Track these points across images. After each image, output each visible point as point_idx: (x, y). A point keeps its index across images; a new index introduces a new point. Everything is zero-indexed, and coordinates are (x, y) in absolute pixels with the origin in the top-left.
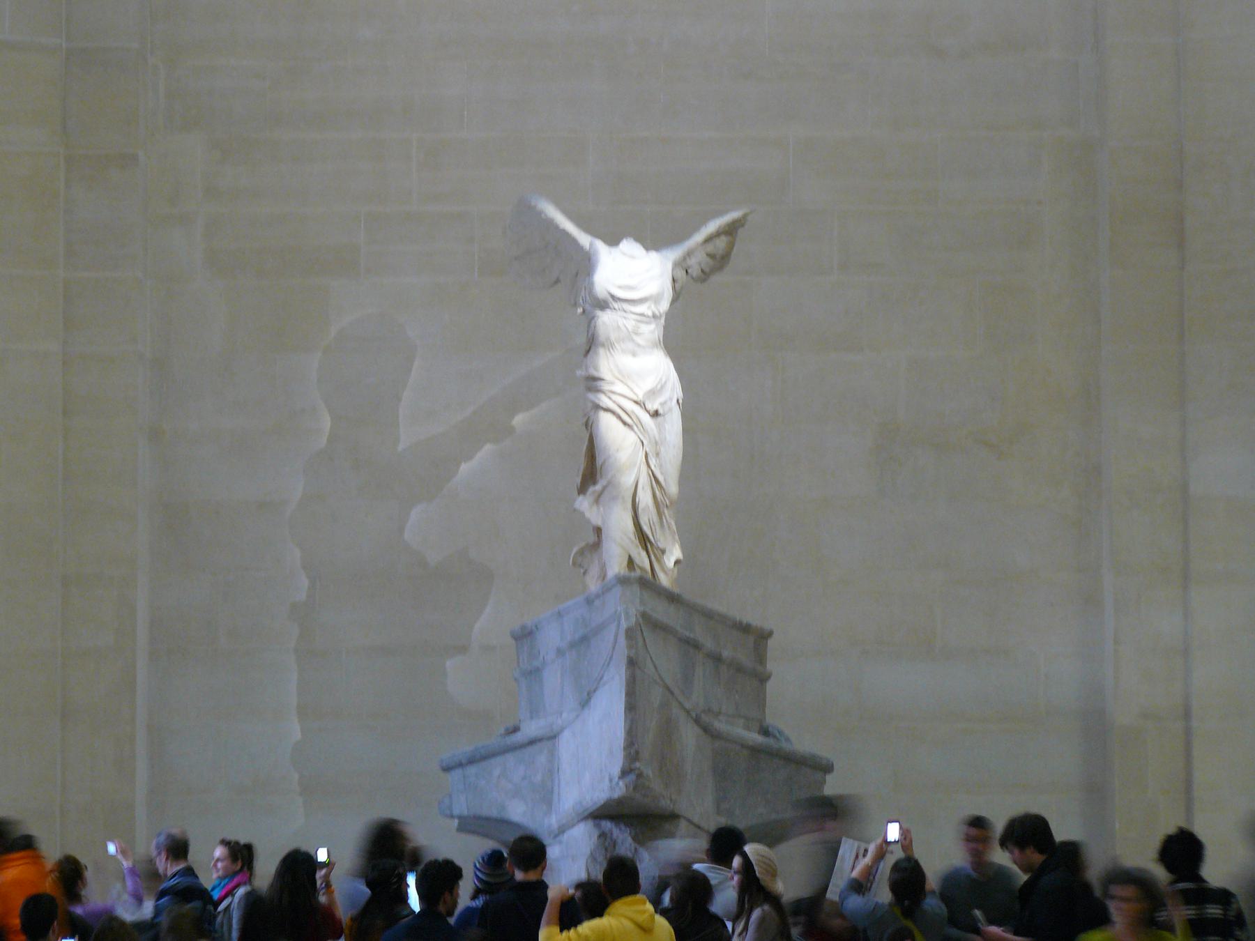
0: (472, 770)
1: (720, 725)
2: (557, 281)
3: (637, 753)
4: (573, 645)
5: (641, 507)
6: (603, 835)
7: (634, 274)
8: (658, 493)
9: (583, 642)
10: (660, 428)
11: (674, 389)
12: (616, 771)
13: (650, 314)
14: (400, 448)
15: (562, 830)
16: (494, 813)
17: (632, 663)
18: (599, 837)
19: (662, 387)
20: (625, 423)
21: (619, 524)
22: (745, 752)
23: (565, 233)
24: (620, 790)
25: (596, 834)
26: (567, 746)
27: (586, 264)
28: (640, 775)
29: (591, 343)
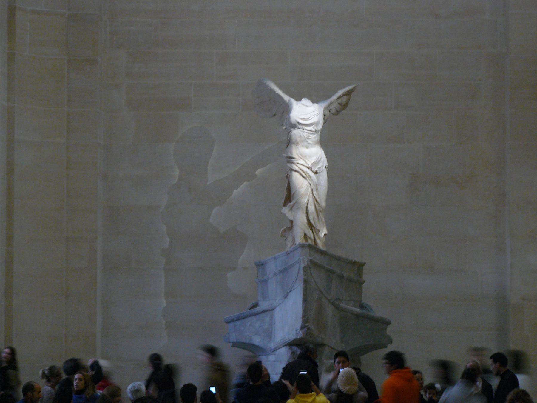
0: (238, 323)
1: (342, 305)
2: (275, 115)
3: (307, 319)
4: (281, 272)
5: (310, 212)
7: (307, 113)
8: (317, 206)
9: (285, 271)
10: (318, 179)
11: (324, 162)
13: (314, 130)
14: (208, 183)
15: (276, 350)
16: (247, 341)
17: (305, 282)
18: (292, 353)
19: (319, 161)
20: (303, 177)
21: (300, 219)
23: (278, 95)
24: (300, 335)
26: (278, 314)
27: (287, 109)
28: (309, 329)
29: (289, 143)
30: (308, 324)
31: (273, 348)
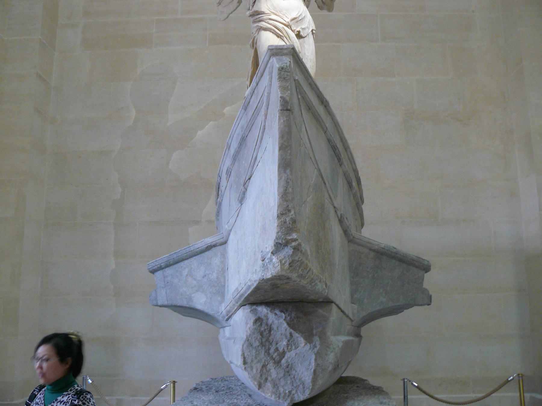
0: (169, 271)
3: (294, 221)
6: (258, 320)
12: (269, 245)
14: (168, 124)
16: (184, 303)
18: (256, 321)
22: (372, 254)
25: (253, 319)
30: (294, 236)
31: (224, 313)
